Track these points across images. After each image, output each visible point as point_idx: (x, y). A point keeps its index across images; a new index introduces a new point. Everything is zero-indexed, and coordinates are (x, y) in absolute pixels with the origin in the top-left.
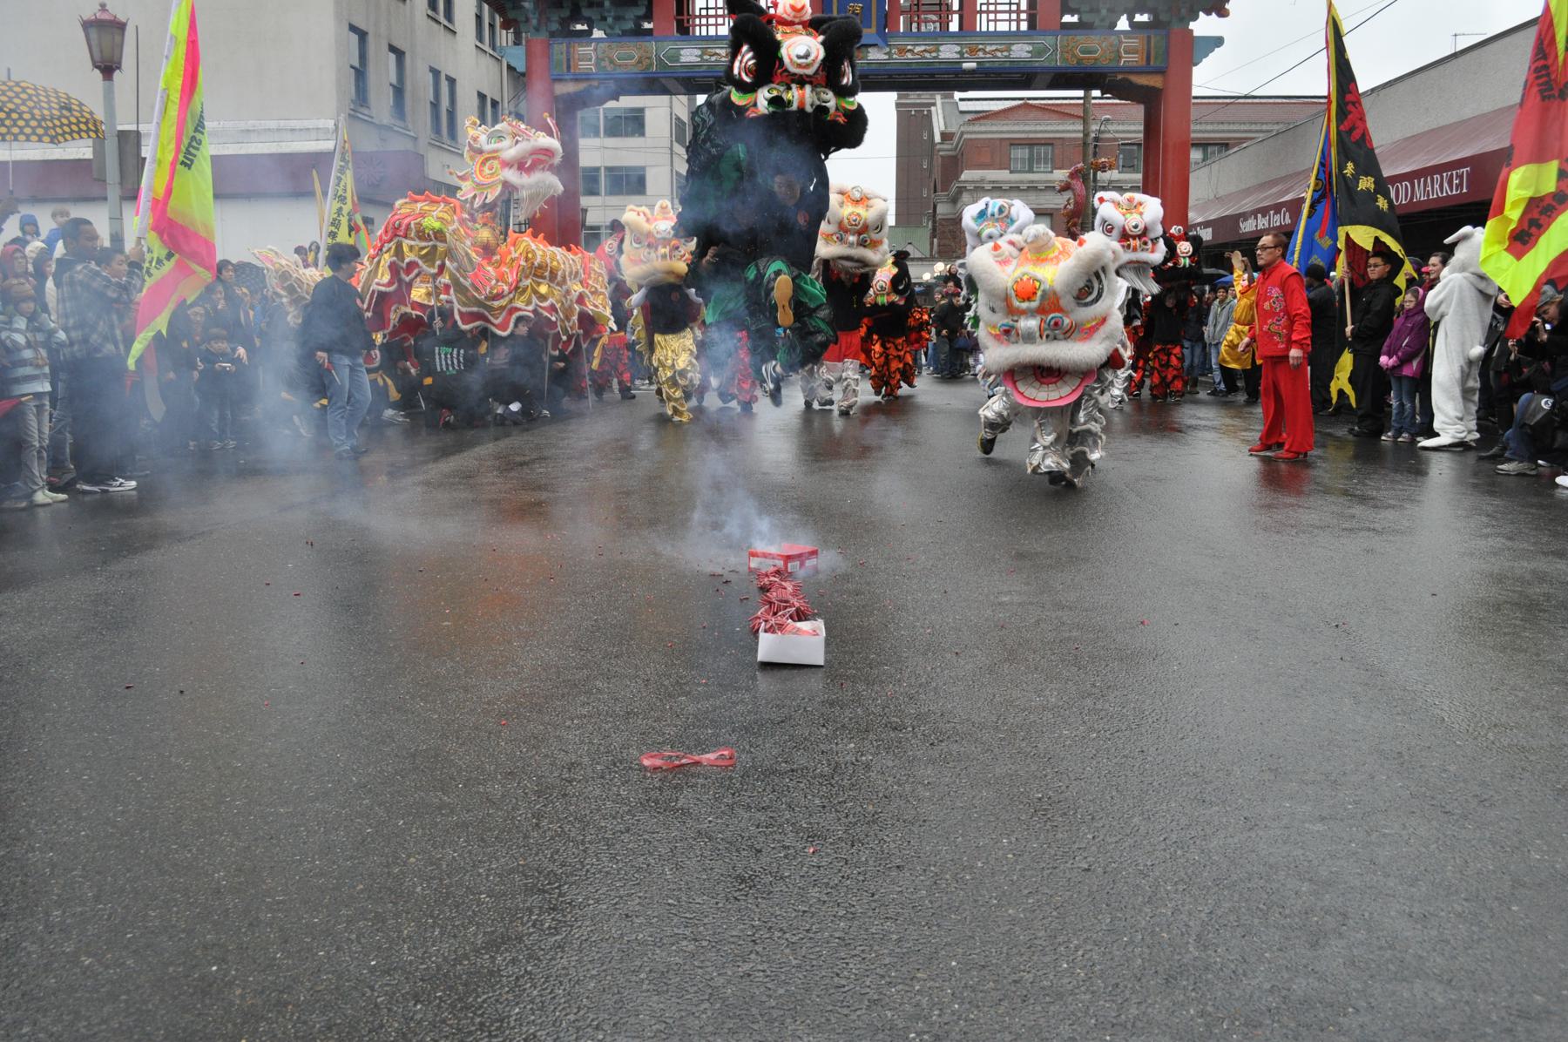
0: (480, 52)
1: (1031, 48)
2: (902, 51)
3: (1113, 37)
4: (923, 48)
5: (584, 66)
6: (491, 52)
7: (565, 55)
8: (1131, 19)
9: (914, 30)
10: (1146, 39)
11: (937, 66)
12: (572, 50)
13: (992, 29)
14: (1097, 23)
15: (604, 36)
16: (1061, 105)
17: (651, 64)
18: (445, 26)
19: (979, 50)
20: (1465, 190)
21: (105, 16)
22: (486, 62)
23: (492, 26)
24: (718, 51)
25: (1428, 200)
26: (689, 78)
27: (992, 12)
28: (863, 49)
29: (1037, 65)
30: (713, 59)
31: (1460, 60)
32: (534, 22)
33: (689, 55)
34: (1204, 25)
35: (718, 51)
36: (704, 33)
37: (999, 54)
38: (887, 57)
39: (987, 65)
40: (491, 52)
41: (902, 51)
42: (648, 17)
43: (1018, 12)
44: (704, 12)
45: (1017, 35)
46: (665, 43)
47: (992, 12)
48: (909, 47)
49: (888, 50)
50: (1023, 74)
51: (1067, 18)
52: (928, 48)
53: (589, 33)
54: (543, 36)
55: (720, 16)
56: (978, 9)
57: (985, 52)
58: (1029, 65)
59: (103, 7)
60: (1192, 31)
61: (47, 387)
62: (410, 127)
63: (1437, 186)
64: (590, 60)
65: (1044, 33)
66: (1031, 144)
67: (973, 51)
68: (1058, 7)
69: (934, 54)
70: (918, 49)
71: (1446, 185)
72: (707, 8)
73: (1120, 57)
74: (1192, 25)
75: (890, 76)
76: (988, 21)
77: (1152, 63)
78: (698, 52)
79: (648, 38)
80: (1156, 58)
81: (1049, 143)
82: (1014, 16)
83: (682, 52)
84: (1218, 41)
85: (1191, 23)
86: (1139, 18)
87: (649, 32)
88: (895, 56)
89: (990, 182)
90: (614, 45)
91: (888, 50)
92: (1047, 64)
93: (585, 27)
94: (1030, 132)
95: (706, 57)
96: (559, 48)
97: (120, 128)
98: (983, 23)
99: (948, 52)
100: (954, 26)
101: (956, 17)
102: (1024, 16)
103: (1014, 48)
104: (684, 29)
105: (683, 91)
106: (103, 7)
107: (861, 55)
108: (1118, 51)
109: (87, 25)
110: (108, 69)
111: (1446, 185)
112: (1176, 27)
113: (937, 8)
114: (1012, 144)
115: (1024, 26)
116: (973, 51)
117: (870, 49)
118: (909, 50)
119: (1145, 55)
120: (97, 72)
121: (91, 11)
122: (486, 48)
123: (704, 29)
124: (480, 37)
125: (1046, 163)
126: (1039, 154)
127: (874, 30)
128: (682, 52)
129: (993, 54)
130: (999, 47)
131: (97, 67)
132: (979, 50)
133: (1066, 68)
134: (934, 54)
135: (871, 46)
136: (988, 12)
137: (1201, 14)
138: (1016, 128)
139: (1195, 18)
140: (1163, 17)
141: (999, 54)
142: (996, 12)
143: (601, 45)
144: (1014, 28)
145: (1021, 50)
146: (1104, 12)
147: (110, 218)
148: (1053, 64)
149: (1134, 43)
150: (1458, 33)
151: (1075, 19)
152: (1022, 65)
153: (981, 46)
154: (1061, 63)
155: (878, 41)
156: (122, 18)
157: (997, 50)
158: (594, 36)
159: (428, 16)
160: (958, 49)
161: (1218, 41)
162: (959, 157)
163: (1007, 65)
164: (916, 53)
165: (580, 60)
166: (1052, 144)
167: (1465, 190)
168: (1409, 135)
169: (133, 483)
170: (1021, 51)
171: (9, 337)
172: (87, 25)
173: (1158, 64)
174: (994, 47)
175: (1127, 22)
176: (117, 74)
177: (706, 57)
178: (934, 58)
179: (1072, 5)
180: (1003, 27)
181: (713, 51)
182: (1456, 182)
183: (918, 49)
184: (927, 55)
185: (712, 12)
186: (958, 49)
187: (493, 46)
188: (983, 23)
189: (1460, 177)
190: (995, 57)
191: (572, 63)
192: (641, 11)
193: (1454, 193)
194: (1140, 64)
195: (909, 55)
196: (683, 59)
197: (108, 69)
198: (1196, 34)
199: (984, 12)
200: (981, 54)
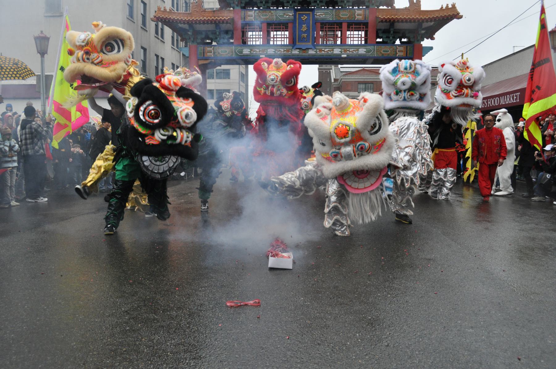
0: (173, 49)
1: (366, 50)
2: (321, 50)
3: (394, 47)
5: (209, 54)
6: (177, 49)
7: (202, 51)
8: (400, 40)
9: (325, 43)
10: (406, 48)
11: (333, 56)
12: (205, 49)
13: (352, 43)
14: (389, 42)
15: (216, 44)
16: (376, 69)
17: (233, 54)
18: (161, 40)
19: (348, 51)
20: (518, 101)
21: (42, 35)
22: (175, 53)
23: (177, 40)
24: (256, 50)
25: (505, 104)
26: (246, 59)
27: (352, 37)
28: (307, 50)
29: (368, 56)
30: (254, 53)
31: (516, 55)
32: (192, 39)
33: (246, 51)
34: (426, 43)
35: (256, 50)
36: (251, 44)
37: (354, 52)
38: (315, 53)
39: (350, 56)
40: (177, 49)
41: (321, 50)
42: (232, 38)
43: (361, 37)
44: (251, 36)
45: (361, 45)
46: (238, 47)
47: (352, 37)
48: (323, 49)
49: (316, 50)
50: (363, 59)
51: (378, 40)
52: (330, 50)
53: (211, 43)
54: (195, 44)
55: (257, 38)
56: (347, 36)
57: (350, 51)
58: (365, 56)
59: (42, 32)
60: (422, 45)
61: (16, 164)
62: (148, 75)
63: (508, 99)
64: (211, 52)
65: (371, 45)
66: (365, 83)
67: (345, 51)
68: (375, 37)
69: (332, 52)
70: (326, 50)
71: (511, 99)
72: (253, 35)
73: (397, 53)
74: (422, 43)
75: (316, 59)
76: (351, 41)
77: (408, 55)
78: (249, 50)
79: (231, 45)
80: (409, 54)
81: (372, 83)
82: (360, 39)
83: (244, 50)
84: (431, 48)
85: (422, 43)
86: (403, 40)
87: (232, 43)
88: (318, 52)
89: (352, 96)
90: (220, 47)
91: (316, 50)
92: (371, 56)
93: (210, 41)
94: (365, 79)
96: (201, 48)
97: (46, 74)
98: (349, 42)
99: (337, 51)
100: (339, 42)
101: (339, 39)
102: (363, 39)
103: (360, 50)
104: (244, 42)
105: (243, 63)
106: (42, 32)
107: (306, 52)
108: (396, 51)
109: (36, 38)
110: (43, 53)
111: (511, 99)
112: (416, 43)
113: (333, 36)
114: (359, 83)
115: (363, 42)
116: (345, 51)
117: (309, 50)
118: (323, 51)
119: (406, 52)
120: (39, 54)
121: (37, 34)
122: (175, 48)
123: (251, 42)
124: (173, 44)
125: (371, 90)
126: (368, 87)
127: (310, 43)
128: (244, 50)
129: (352, 52)
130: (354, 50)
131: (39, 53)
132: (348, 51)
133: (378, 57)
134: (332, 52)
136: (351, 37)
137: (425, 39)
138: (360, 77)
139: (423, 40)
140: (412, 40)
141: (354, 52)
142: (353, 37)
143: (215, 47)
144: (360, 43)
145: (362, 51)
146: (391, 38)
147: (42, 105)
148: (373, 56)
149: (401, 48)
150: (515, 46)
151: (381, 40)
152: (362, 56)
153: (348, 49)
154: (376, 55)
155: (312, 47)
156: (48, 36)
157: (354, 51)
158: (213, 44)
159: (155, 36)
160: (340, 50)
161: (431, 48)
162: (340, 87)
163: (357, 56)
164: (326, 51)
165: (208, 52)
166: (373, 83)
167: (518, 101)
168: (498, 81)
169: (46, 199)
170: (362, 51)
171: (3, 147)
172: (36, 38)
173: (410, 56)
174: (353, 50)
175: (399, 42)
176: (46, 55)
177: (252, 52)
178: (332, 53)
179: (380, 35)
180: (356, 43)
181: (255, 50)
182: (515, 98)
183: (326, 50)
184: (329, 52)
185: (254, 36)
186: (340, 50)
187: (178, 47)
188: (349, 42)
189: (516, 96)
190: (353, 53)
191: (205, 54)
192: (230, 36)
193: (514, 101)
194: (404, 56)
195: (323, 52)
196: (244, 53)
197: (43, 53)
198: (423, 46)
199: (349, 37)
200: (348, 52)
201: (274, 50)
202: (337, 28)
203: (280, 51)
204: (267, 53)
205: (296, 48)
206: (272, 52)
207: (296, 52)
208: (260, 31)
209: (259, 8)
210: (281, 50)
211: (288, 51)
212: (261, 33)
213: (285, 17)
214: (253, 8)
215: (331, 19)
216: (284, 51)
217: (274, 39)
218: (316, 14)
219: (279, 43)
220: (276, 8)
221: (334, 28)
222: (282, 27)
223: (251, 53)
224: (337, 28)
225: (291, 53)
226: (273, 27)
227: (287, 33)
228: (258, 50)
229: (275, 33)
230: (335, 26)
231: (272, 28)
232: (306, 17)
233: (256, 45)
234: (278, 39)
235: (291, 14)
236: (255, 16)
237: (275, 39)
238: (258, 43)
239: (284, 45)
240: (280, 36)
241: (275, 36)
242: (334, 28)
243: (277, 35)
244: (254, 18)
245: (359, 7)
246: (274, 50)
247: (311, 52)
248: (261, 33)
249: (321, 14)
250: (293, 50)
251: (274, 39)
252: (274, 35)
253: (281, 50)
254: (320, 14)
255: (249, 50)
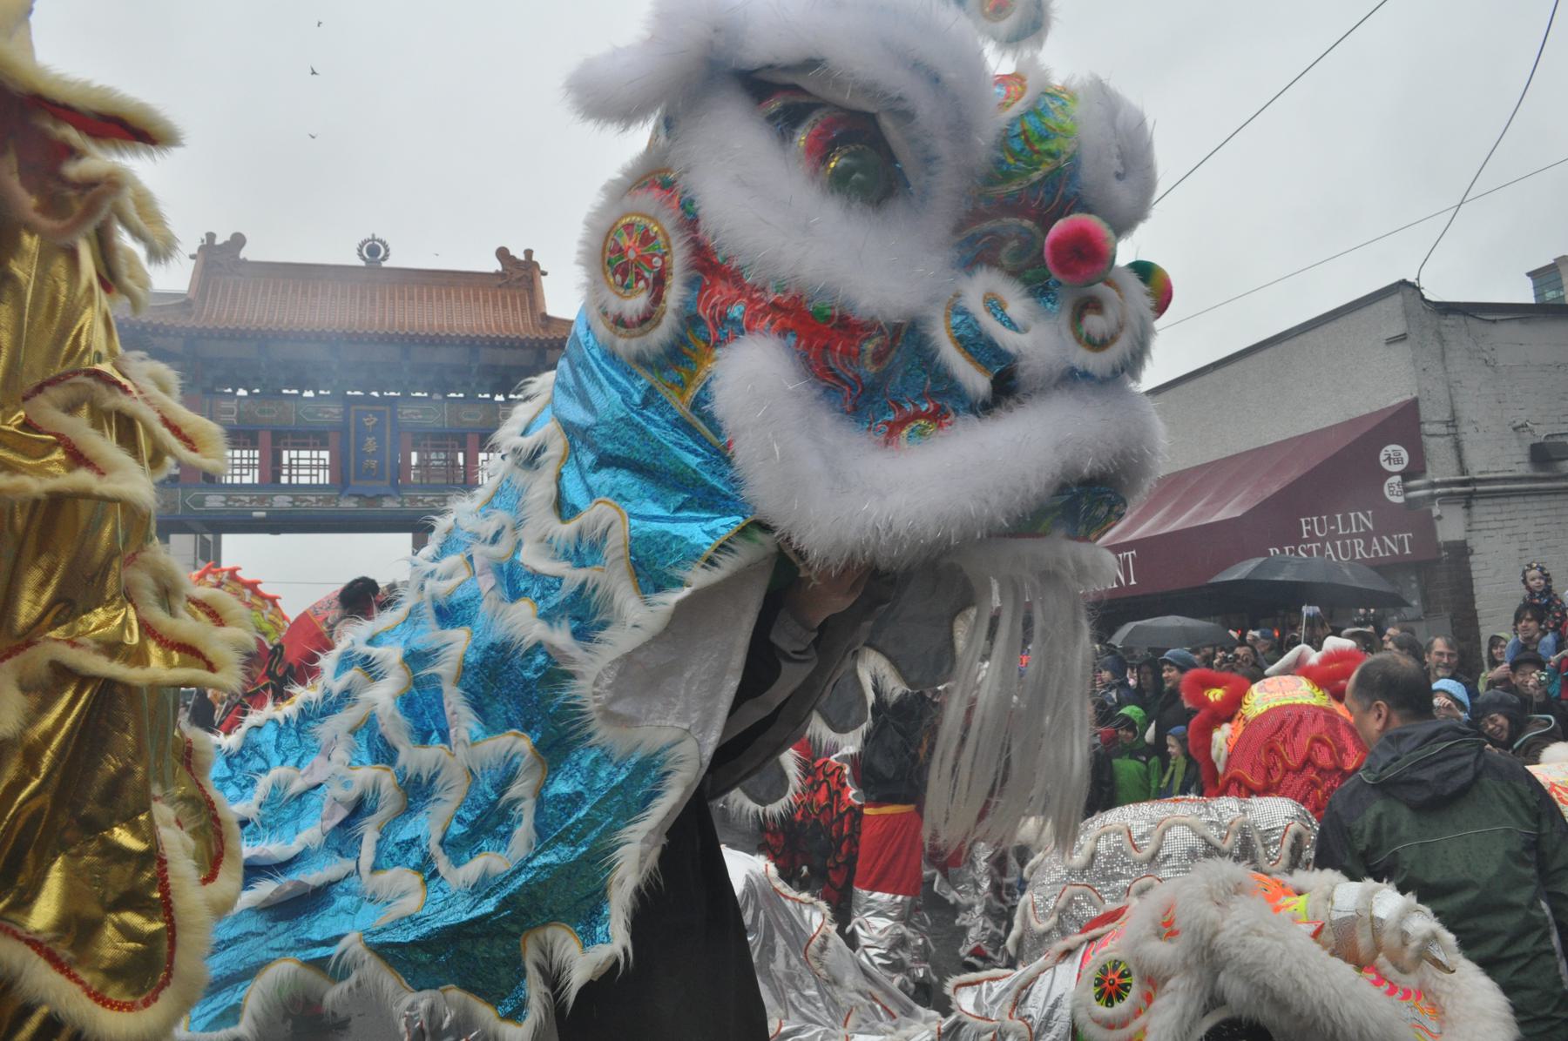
2: (413, 500)
4: (431, 498)
17: (177, 509)
24: (242, 498)
33: (214, 501)
36: (229, 481)
41: (413, 500)
49: (400, 499)
70: (427, 499)
78: (223, 499)
83: (207, 498)
91: (400, 499)
95: (230, 503)
117: (384, 499)
118: (420, 500)
135: (384, 496)
183: (427, 499)
184: (436, 504)
195: (420, 504)
196: (208, 504)
201: (291, 499)
202: (453, 446)
203: (307, 500)
204: (271, 506)
205: (350, 495)
206: (286, 505)
207: (349, 504)
208: (254, 450)
209: (250, 393)
210: (309, 498)
211: (328, 500)
212: (257, 453)
213: (320, 418)
214: (235, 390)
215: (439, 425)
216: (318, 501)
217: (290, 472)
218: (401, 413)
219: (304, 480)
220: (295, 392)
221: (447, 446)
222: (311, 441)
223: (227, 506)
224: (453, 446)
225: (337, 507)
226: (289, 441)
227: (325, 454)
228: (247, 499)
229: (294, 454)
230: (450, 443)
231: (286, 444)
232: (375, 419)
233: (242, 487)
234: (301, 472)
235: (336, 411)
236: (239, 413)
237: (294, 472)
238: (247, 480)
239: (318, 487)
240: (308, 462)
241: (294, 462)
242: (447, 446)
243: (298, 459)
244: (238, 417)
245: (506, 396)
246: (291, 499)
247: (389, 504)
248: (257, 453)
249: (412, 413)
250: (341, 499)
251: (290, 472)
252: (290, 460)
253: (309, 498)
254: (410, 411)
255: (223, 499)
